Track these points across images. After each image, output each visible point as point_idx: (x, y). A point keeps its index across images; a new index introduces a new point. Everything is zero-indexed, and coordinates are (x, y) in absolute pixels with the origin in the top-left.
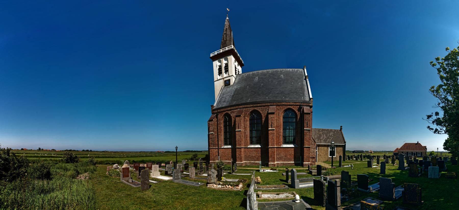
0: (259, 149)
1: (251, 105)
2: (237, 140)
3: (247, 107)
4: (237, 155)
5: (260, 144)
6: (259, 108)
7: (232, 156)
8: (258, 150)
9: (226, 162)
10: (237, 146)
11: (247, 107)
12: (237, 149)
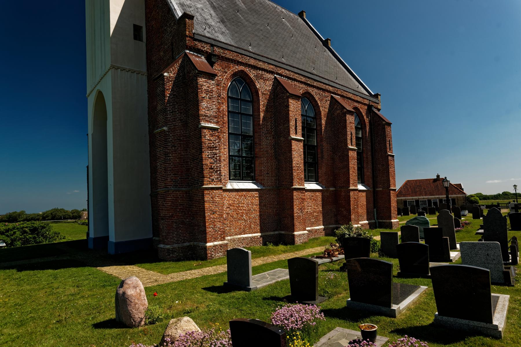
0: (318, 194)
1: (302, 77)
2: (294, 165)
3: (295, 80)
4: (295, 210)
6: (316, 93)
7: (260, 215)
8: (317, 196)
9: (244, 239)
10: (295, 182)
11: (295, 80)
12: (295, 193)
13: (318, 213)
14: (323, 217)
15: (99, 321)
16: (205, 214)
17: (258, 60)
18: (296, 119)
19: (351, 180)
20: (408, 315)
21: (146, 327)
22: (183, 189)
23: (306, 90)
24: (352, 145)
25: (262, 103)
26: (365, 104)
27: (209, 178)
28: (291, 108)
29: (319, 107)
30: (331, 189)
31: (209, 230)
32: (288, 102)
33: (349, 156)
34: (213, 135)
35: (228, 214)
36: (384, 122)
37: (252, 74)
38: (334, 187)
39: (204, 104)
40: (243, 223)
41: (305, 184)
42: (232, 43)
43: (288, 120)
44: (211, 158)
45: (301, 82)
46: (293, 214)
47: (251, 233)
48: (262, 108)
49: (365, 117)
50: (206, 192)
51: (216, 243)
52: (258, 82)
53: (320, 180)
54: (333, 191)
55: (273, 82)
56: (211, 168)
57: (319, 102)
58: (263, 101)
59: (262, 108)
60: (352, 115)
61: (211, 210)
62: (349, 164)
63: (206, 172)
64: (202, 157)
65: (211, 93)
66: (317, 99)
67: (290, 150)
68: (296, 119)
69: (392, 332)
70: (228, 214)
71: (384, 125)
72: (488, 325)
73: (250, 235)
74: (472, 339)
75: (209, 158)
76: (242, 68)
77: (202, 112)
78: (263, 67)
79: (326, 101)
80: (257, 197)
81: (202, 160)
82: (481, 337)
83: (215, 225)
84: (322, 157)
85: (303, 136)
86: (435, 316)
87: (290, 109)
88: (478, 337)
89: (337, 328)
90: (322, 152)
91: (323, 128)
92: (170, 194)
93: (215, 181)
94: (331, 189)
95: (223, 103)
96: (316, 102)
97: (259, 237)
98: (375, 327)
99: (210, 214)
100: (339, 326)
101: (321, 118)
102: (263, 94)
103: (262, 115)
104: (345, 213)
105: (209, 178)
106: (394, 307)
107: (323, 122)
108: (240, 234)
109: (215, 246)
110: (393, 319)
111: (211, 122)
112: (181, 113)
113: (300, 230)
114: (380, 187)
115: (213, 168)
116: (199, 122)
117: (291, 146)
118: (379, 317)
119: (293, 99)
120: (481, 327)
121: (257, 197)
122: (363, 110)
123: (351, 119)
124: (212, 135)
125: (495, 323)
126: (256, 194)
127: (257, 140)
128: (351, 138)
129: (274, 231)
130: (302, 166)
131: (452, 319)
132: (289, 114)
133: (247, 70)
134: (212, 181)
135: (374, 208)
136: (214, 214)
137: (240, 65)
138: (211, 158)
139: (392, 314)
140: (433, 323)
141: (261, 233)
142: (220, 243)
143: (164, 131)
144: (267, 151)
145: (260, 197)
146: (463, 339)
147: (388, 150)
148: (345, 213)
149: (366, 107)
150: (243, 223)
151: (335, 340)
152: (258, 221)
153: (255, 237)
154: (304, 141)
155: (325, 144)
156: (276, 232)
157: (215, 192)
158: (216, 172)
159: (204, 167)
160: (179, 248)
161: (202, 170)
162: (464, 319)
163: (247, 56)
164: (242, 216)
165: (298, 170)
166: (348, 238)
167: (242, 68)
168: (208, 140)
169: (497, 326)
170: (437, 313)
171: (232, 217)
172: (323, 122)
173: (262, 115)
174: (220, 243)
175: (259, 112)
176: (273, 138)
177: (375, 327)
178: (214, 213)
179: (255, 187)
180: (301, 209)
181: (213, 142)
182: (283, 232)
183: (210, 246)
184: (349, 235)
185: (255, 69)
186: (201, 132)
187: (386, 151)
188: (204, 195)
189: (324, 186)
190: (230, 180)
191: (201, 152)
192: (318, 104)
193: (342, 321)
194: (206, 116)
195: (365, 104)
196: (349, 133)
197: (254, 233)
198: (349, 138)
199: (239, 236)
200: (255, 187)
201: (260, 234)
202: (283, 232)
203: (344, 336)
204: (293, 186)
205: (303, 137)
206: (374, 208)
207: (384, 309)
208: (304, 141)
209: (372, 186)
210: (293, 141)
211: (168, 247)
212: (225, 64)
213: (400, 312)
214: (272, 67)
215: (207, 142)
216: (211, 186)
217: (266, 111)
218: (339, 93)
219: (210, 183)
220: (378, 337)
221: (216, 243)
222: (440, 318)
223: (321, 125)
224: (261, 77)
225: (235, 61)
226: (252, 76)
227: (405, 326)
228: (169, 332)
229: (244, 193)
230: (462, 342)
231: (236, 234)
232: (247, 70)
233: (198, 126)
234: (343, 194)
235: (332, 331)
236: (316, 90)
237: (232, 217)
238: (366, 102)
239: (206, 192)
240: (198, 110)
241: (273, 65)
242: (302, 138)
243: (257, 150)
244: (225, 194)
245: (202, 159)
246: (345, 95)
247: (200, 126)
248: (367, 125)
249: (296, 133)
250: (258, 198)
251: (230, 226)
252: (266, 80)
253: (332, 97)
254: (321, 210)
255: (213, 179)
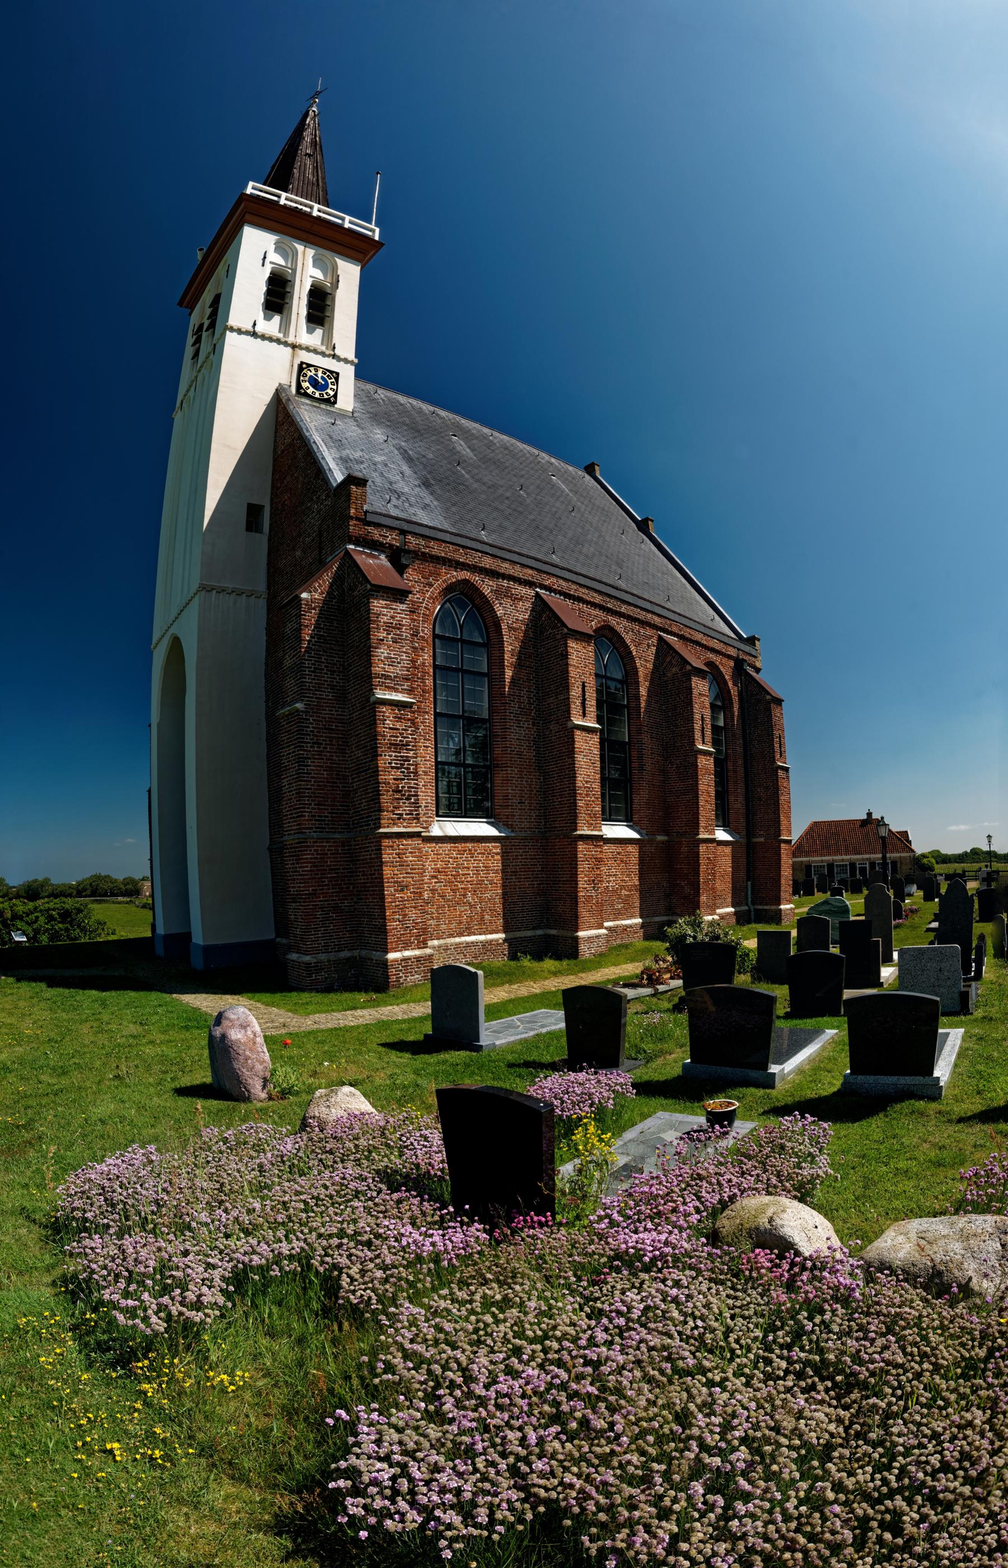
0: (630, 848)
1: (595, 595)
2: (579, 784)
3: (580, 600)
4: (580, 885)
5: (629, 820)
7: (504, 894)
9: (468, 945)
10: (581, 823)
11: (580, 600)
12: (581, 846)
13: (630, 891)
14: (641, 898)
15: (183, 1085)
16: (384, 890)
17: (501, 558)
18: (584, 683)
19: (701, 818)
20: (797, 1081)
21: (271, 1103)
22: (336, 836)
23: (604, 621)
24: (703, 743)
25: (508, 648)
26: (729, 657)
27: (393, 811)
28: (574, 659)
29: (632, 658)
30: (660, 838)
31: (391, 925)
32: (566, 646)
33: (697, 766)
34: (400, 718)
35: (433, 891)
36: (768, 697)
37: (487, 587)
38: (667, 834)
39: (382, 652)
40: (466, 910)
41: (603, 827)
42: (446, 526)
43: (565, 685)
44: (397, 768)
45: (594, 605)
46: (577, 892)
47: (485, 933)
48: (509, 659)
49: (730, 684)
50: (386, 842)
51: (407, 953)
52: (501, 604)
53: (636, 817)
54: (663, 842)
55: (533, 603)
56: (397, 791)
57: (633, 648)
58: (511, 644)
59: (509, 659)
60: (704, 678)
61: (397, 882)
62: (697, 784)
63: (386, 799)
64: (377, 767)
65: (399, 629)
66: (628, 641)
67: (571, 752)
68: (584, 683)
69: (764, 1113)
70: (433, 891)
71: (769, 703)
72: (927, 1080)
73: (482, 938)
74: (898, 1107)
75: (392, 768)
76: (465, 575)
77: (377, 669)
78: (511, 572)
79: (648, 645)
80: (497, 854)
81: (376, 772)
82: (913, 1101)
83: (405, 915)
84: (641, 768)
85: (599, 720)
86: (845, 1076)
87: (571, 662)
88: (907, 1103)
89: (660, 1114)
90: (641, 757)
91: (643, 705)
92: (308, 846)
93: (404, 819)
94: (660, 838)
95: (423, 649)
96: (627, 647)
97: (501, 941)
98: (733, 1104)
99: (395, 890)
100: (664, 1110)
101: (637, 683)
102: (510, 628)
103: (509, 673)
104: (687, 890)
105: (393, 811)
106: (774, 1069)
107: (643, 691)
108: (461, 934)
109: (405, 960)
110: (768, 1091)
111: (396, 691)
112: (333, 672)
113: (590, 928)
114: (760, 836)
115: (400, 791)
116: (371, 691)
117: (574, 742)
118: (744, 1090)
119: (576, 639)
120: (915, 1085)
121: (497, 854)
122: (727, 669)
123: (700, 687)
124: (399, 719)
125: (937, 1073)
126: (496, 848)
127: (498, 730)
128: (703, 728)
129: (534, 928)
130: (597, 786)
131: (871, 1079)
132: (567, 672)
133: (476, 579)
134: (399, 819)
135: (748, 880)
136: (402, 890)
137: (462, 570)
138: (397, 768)
139: (769, 1082)
140: (839, 1090)
141: (505, 932)
142: (417, 952)
143: (298, 710)
144: (520, 754)
145: (505, 855)
146: (884, 1109)
147: (778, 756)
148: (687, 890)
149: (732, 663)
150: (466, 910)
151: (654, 1133)
152: (499, 908)
153: (491, 941)
154: (602, 731)
155: (646, 738)
156: (539, 932)
157: (405, 842)
158: (408, 799)
159: (382, 787)
160: (329, 961)
161: (378, 794)
162: (891, 1075)
163: (477, 551)
164: (465, 896)
165: (587, 795)
166: (691, 944)
167: (465, 575)
168: (390, 728)
169: (938, 1078)
170: (849, 1071)
171: (443, 897)
172: (643, 691)
173: (509, 673)
174: (417, 952)
175: (502, 666)
176: (533, 724)
177: (733, 1104)
178: (403, 888)
179: (491, 831)
180: (594, 882)
181: (401, 734)
182: (553, 932)
183: (396, 960)
184: (695, 938)
185: (493, 577)
186: (375, 711)
187: (774, 757)
188: (381, 849)
189: (644, 832)
190: (438, 816)
191: (375, 756)
192: (631, 652)
193: (670, 1102)
194: (387, 677)
195: (729, 657)
196: (697, 716)
197: (491, 933)
198: (697, 726)
199: (458, 940)
200: (491, 831)
201: (503, 936)
202: (553, 932)
203: (671, 1126)
204: (576, 830)
205: (598, 723)
206: (748, 880)
207: (754, 1074)
208: (602, 731)
209: (744, 833)
210: (578, 732)
211: (307, 958)
212: (430, 567)
213: (784, 1077)
214: (530, 572)
215: (388, 734)
216: (395, 830)
217: (518, 666)
218: (675, 629)
219: (394, 824)
220: (737, 1123)
221: (407, 953)
222: (852, 1079)
223: (637, 697)
224: (507, 594)
225: (450, 561)
226: (487, 591)
227: (789, 1100)
228: (314, 1111)
229: (470, 845)
230: (881, 1115)
231: (451, 936)
232: (476, 579)
233: (368, 700)
234: (684, 849)
235: (649, 1120)
236: (625, 622)
237: (443, 897)
238: (732, 652)
239: (386, 842)
240: (369, 664)
241: (532, 568)
242: (597, 726)
243: (498, 751)
244: (427, 848)
245: (378, 771)
246: (688, 636)
247: (372, 699)
248: (736, 699)
249: (584, 715)
250: (499, 857)
251: (438, 918)
252: (516, 599)
253: (660, 638)
254: (637, 883)
255: (402, 815)
